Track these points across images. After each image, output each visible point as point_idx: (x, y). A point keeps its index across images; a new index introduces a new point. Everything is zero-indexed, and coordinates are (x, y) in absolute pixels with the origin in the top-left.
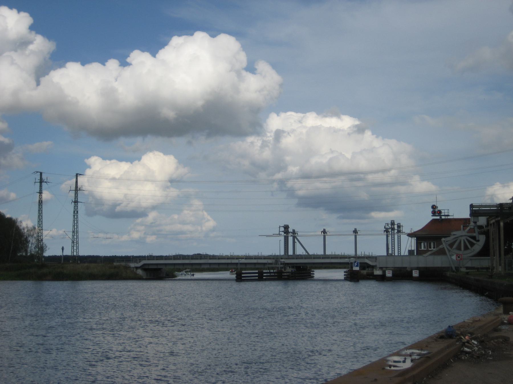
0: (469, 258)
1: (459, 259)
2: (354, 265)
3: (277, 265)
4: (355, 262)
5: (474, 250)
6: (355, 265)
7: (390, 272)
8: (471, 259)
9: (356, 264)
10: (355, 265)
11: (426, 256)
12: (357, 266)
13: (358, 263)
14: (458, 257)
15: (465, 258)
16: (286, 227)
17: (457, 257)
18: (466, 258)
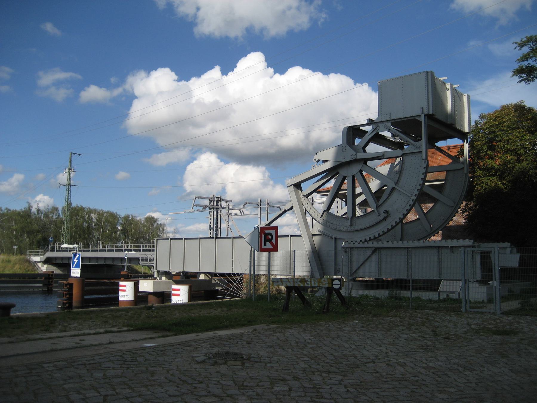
0: (370, 244)
1: (269, 245)
2: (74, 262)
3: (148, 262)
4: (75, 255)
5: (386, 212)
6: (75, 262)
7: (124, 286)
8: (376, 250)
9: (76, 260)
10: (75, 262)
12: (77, 266)
13: (78, 259)
15: (357, 245)
16: (212, 198)
18: (361, 245)
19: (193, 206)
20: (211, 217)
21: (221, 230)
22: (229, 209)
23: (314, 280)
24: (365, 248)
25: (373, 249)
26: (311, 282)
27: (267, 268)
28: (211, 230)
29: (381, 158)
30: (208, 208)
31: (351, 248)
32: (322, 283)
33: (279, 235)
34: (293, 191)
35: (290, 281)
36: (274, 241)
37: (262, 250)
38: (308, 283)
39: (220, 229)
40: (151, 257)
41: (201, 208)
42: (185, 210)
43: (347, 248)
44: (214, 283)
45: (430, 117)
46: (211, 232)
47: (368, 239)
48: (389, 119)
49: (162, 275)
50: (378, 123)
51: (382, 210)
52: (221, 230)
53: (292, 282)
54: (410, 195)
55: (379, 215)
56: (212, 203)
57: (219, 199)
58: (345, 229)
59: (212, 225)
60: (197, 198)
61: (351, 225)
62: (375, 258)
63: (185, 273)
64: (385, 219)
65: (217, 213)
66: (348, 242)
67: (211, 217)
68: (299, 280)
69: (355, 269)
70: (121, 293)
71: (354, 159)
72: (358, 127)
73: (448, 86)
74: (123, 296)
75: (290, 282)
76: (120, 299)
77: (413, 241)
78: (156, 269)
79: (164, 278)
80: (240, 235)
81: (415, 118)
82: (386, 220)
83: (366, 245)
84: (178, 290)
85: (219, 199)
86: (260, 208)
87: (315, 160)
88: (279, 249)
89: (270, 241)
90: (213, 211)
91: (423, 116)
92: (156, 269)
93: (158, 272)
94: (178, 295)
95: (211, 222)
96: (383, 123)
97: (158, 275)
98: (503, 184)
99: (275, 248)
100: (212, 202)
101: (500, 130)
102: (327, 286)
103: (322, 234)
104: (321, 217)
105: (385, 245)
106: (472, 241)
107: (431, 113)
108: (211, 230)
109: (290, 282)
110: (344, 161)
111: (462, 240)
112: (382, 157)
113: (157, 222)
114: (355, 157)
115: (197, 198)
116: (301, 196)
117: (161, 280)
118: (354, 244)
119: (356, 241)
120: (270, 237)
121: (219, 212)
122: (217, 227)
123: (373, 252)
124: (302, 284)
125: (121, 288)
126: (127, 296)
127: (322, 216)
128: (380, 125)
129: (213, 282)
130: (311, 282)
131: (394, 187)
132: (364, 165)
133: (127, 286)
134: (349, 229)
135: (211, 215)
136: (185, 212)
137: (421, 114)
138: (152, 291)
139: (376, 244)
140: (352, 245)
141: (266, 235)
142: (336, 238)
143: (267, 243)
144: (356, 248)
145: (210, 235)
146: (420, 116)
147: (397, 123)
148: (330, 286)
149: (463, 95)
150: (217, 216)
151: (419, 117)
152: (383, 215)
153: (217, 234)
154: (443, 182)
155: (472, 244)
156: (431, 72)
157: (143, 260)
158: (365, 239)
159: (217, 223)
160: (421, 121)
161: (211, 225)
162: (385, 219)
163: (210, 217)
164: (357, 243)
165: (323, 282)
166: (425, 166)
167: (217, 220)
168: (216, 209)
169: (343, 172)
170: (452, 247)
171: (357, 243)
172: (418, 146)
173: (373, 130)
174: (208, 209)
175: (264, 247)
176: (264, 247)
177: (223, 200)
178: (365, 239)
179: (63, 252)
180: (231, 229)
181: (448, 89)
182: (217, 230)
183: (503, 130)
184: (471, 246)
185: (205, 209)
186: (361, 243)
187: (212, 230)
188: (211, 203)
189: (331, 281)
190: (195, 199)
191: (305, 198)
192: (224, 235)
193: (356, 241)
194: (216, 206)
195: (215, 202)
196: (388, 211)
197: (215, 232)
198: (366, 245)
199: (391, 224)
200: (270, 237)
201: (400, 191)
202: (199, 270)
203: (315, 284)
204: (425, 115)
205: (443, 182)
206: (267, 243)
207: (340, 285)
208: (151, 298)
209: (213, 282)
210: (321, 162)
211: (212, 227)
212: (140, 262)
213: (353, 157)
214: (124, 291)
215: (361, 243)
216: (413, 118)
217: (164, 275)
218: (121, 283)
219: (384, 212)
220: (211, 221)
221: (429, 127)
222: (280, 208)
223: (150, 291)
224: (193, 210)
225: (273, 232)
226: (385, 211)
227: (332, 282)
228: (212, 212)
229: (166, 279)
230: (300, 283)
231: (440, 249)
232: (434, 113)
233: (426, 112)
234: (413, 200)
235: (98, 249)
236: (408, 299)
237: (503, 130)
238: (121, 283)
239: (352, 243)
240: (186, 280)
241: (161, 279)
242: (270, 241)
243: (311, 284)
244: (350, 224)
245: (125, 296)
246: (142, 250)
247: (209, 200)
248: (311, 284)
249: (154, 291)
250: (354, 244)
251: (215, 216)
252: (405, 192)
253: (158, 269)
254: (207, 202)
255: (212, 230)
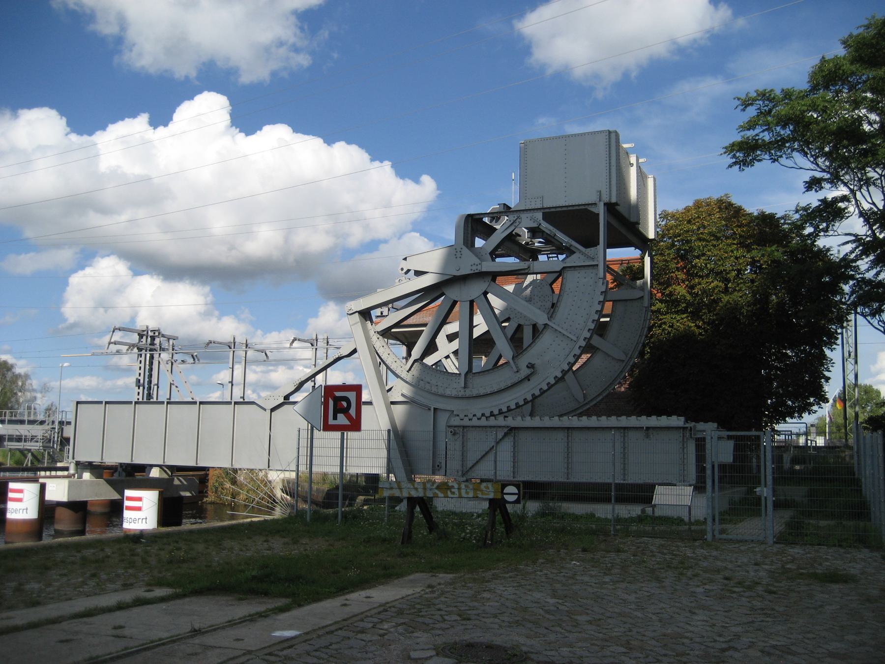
0: (501, 421)
1: (342, 419)
3: (22, 444)
5: (531, 366)
7: (21, 491)
8: (512, 430)
11: (273, 410)
14: (337, 400)
15: (475, 422)
16: (144, 331)
17: (331, 403)
18: (484, 422)
19: (109, 344)
20: (140, 365)
21: (158, 387)
22: (175, 352)
23: (465, 486)
24: (491, 427)
25: (506, 430)
26: (459, 489)
27: (338, 461)
28: (139, 388)
29: (523, 272)
30: (136, 348)
31: (464, 427)
32: (482, 491)
33: (363, 400)
34: (358, 323)
35: (416, 486)
36: (353, 412)
37: (327, 427)
38: (453, 490)
39: (156, 387)
40: (27, 433)
41: (124, 348)
42: (94, 351)
43: (455, 427)
44: (177, 486)
45: (611, 207)
46: (139, 391)
47: (496, 412)
48: (539, 206)
49: (84, 469)
50: (518, 213)
51: (523, 361)
52: (158, 387)
53: (419, 490)
54: (574, 338)
55: (517, 372)
56: (144, 339)
57: (157, 334)
58: (454, 393)
59: (141, 378)
60: (117, 329)
61: (465, 387)
62: (506, 447)
63: (126, 466)
64: (528, 378)
65: (152, 357)
66: (458, 415)
67: (140, 365)
68: (435, 486)
69: (470, 465)
70: (10, 505)
71: (476, 271)
72: (481, 216)
73: (633, 159)
74: (16, 511)
75: (416, 489)
76: (9, 516)
77: (551, 417)
78: (73, 458)
79: (87, 476)
80: (193, 399)
81: (586, 207)
82: (529, 380)
83: (492, 422)
84: (139, 499)
85: (157, 334)
86: (234, 352)
87: (402, 269)
88: (363, 427)
89: (346, 411)
90: (146, 355)
91: (602, 204)
92: (73, 458)
93: (78, 464)
94: (139, 509)
95: (140, 374)
96: (529, 212)
97: (77, 469)
98: (698, 327)
99: (355, 425)
100: (145, 338)
101: (700, 239)
102: (491, 496)
103: (410, 402)
104: (408, 372)
105: (529, 422)
106: (682, 419)
107: (614, 200)
108: (139, 388)
109: (416, 489)
110: (458, 274)
111: (665, 417)
112: (526, 271)
113: (13, 370)
114: (479, 267)
115: (117, 329)
116: (372, 333)
117: (82, 478)
118: (470, 420)
119: (474, 415)
120: (345, 404)
121: (156, 356)
122: (150, 382)
123: (506, 435)
124: (442, 493)
125: (11, 495)
126: (25, 511)
127: (410, 369)
128: (524, 216)
129: (176, 482)
130: (459, 489)
131: (546, 324)
132: (492, 283)
133: (25, 492)
134: (461, 394)
135: (141, 361)
136: (93, 354)
137: (597, 202)
138: (65, 499)
139: (510, 422)
140: (466, 422)
141: (337, 400)
142: (435, 409)
143: (338, 415)
144: (473, 427)
145: (138, 397)
146: (595, 204)
147: (553, 216)
148: (499, 496)
149: (646, 177)
150: (151, 363)
151: (593, 206)
152: (525, 372)
153: (149, 396)
154: (608, 319)
155: (683, 423)
156: (616, 132)
157: (11, 439)
158: (492, 412)
159: (150, 376)
160: (598, 214)
161: (139, 378)
162: (528, 378)
163: (138, 365)
164: (475, 419)
165: (484, 489)
166: (604, 290)
167: (151, 370)
168: (150, 351)
169: (453, 293)
170: (648, 428)
171: (475, 419)
172: (592, 256)
173: (510, 223)
174: (136, 350)
175: (331, 421)
176: (331, 421)
177: (163, 336)
178: (492, 412)
179: (28, 424)
180: (177, 387)
181: (632, 165)
182: (149, 388)
183: (704, 240)
184: (680, 428)
185: (132, 350)
186: (484, 418)
187: (141, 388)
188: (142, 340)
189: (500, 487)
190: (113, 331)
191: (379, 336)
192: (163, 396)
193: (474, 415)
194: (150, 345)
195: (149, 339)
196: (534, 364)
197: (146, 392)
198: (492, 422)
199: (540, 388)
200: (345, 404)
201: (556, 330)
202: (164, 462)
203: (467, 493)
204: (605, 204)
205: (608, 319)
206: (338, 415)
207: (519, 494)
208: (60, 512)
209: (176, 482)
210: (412, 273)
211: (142, 381)
212: (6, 443)
213: (474, 268)
214: (20, 500)
215: (484, 418)
216: (583, 207)
217: (89, 470)
218: (12, 485)
219: (527, 367)
220: (140, 371)
221: (609, 226)
222: (266, 354)
223: (60, 500)
224: (109, 351)
225: (352, 396)
226: (529, 363)
227: (503, 488)
228: (143, 356)
229: (92, 477)
230: (437, 491)
231: (626, 431)
232: (619, 202)
233: (605, 199)
234: (580, 347)
235: (26, 418)
236: (576, 518)
237: (704, 240)
238: (12, 485)
239: (466, 419)
240: (128, 478)
241: (80, 477)
242: (346, 411)
243: (460, 493)
244: (463, 386)
245: (21, 511)
246: (8, 420)
247: (139, 334)
248: (460, 493)
249: (72, 499)
250: (470, 420)
251: (147, 363)
252: (565, 333)
253: (78, 459)
254: (135, 338)
255: (141, 388)
